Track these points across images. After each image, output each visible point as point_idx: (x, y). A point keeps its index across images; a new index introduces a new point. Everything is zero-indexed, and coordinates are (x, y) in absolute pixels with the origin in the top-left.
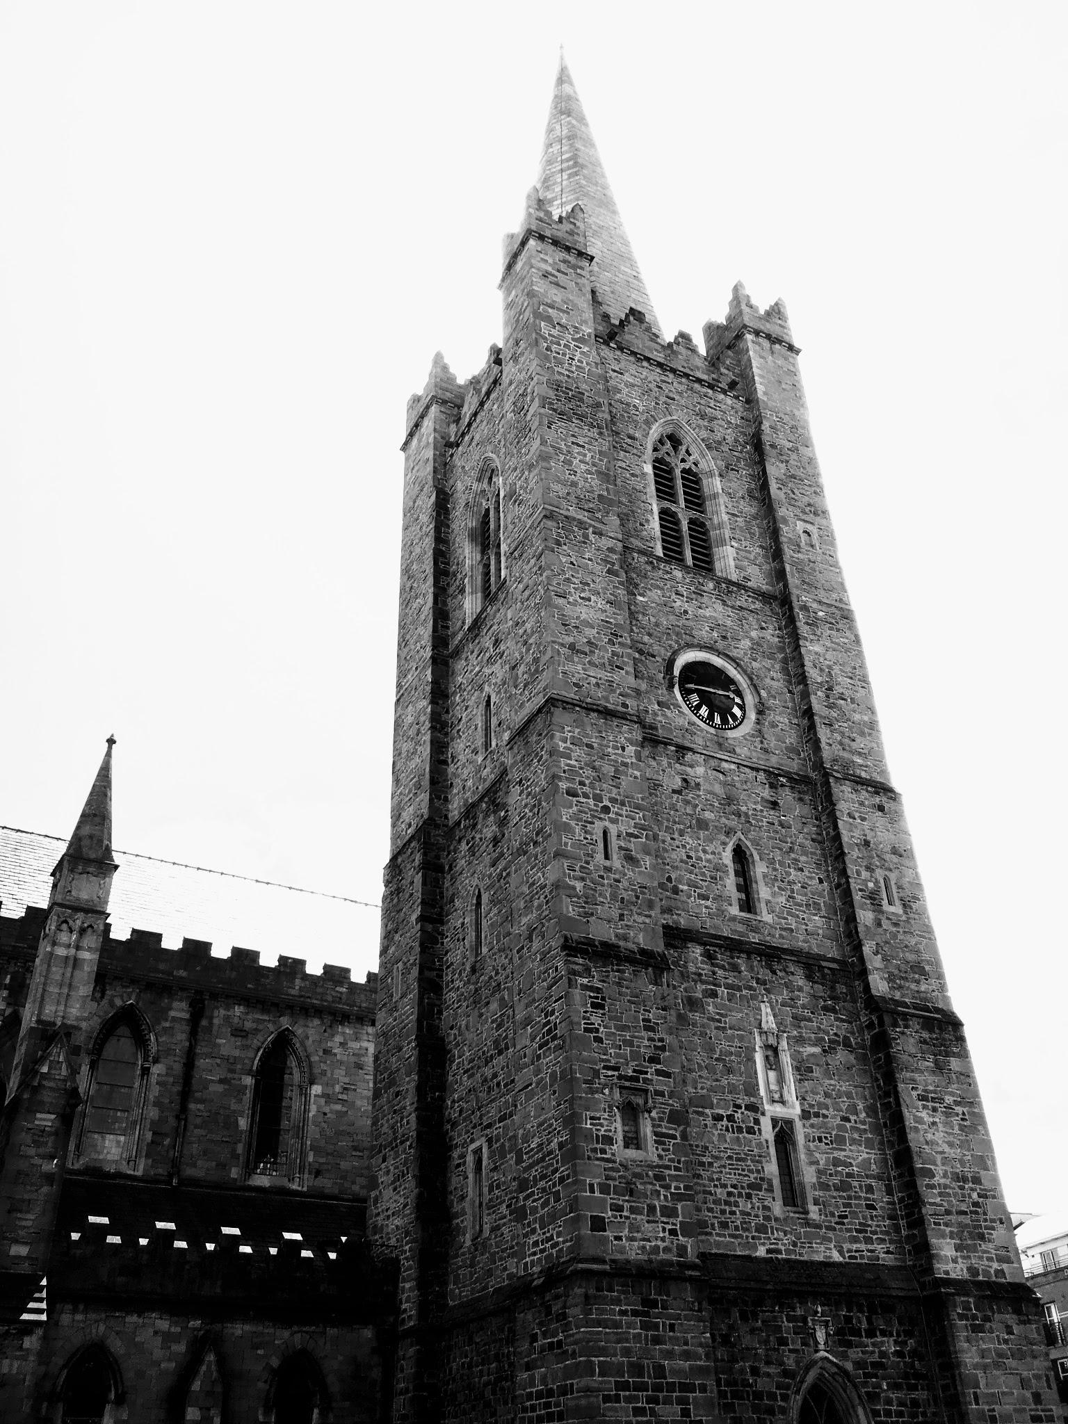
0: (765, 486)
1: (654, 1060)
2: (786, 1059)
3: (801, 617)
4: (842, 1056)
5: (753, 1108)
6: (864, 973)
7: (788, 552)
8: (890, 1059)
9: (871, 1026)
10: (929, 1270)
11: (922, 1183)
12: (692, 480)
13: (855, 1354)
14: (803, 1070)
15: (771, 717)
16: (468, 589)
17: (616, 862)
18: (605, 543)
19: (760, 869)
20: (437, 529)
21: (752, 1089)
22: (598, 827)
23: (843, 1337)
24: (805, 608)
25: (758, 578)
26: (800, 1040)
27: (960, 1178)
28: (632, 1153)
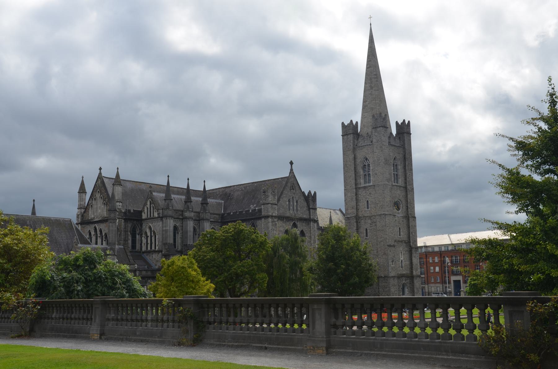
0: (405, 166)
1: (394, 256)
2: (402, 253)
3: (408, 191)
4: (407, 252)
5: (400, 259)
6: (410, 243)
7: (407, 179)
8: (412, 253)
9: (410, 249)
10: (413, 274)
11: (413, 265)
12: (396, 165)
13: (406, 282)
14: (404, 254)
15: (403, 207)
16: (362, 178)
17: (391, 234)
18: (390, 186)
19: (401, 230)
20: (355, 163)
21: (400, 257)
22: (389, 230)
23: (405, 280)
24: (408, 189)
25: (403, 185)
26: (404, 251)
27: (416, 265)
28: (392, 266)
